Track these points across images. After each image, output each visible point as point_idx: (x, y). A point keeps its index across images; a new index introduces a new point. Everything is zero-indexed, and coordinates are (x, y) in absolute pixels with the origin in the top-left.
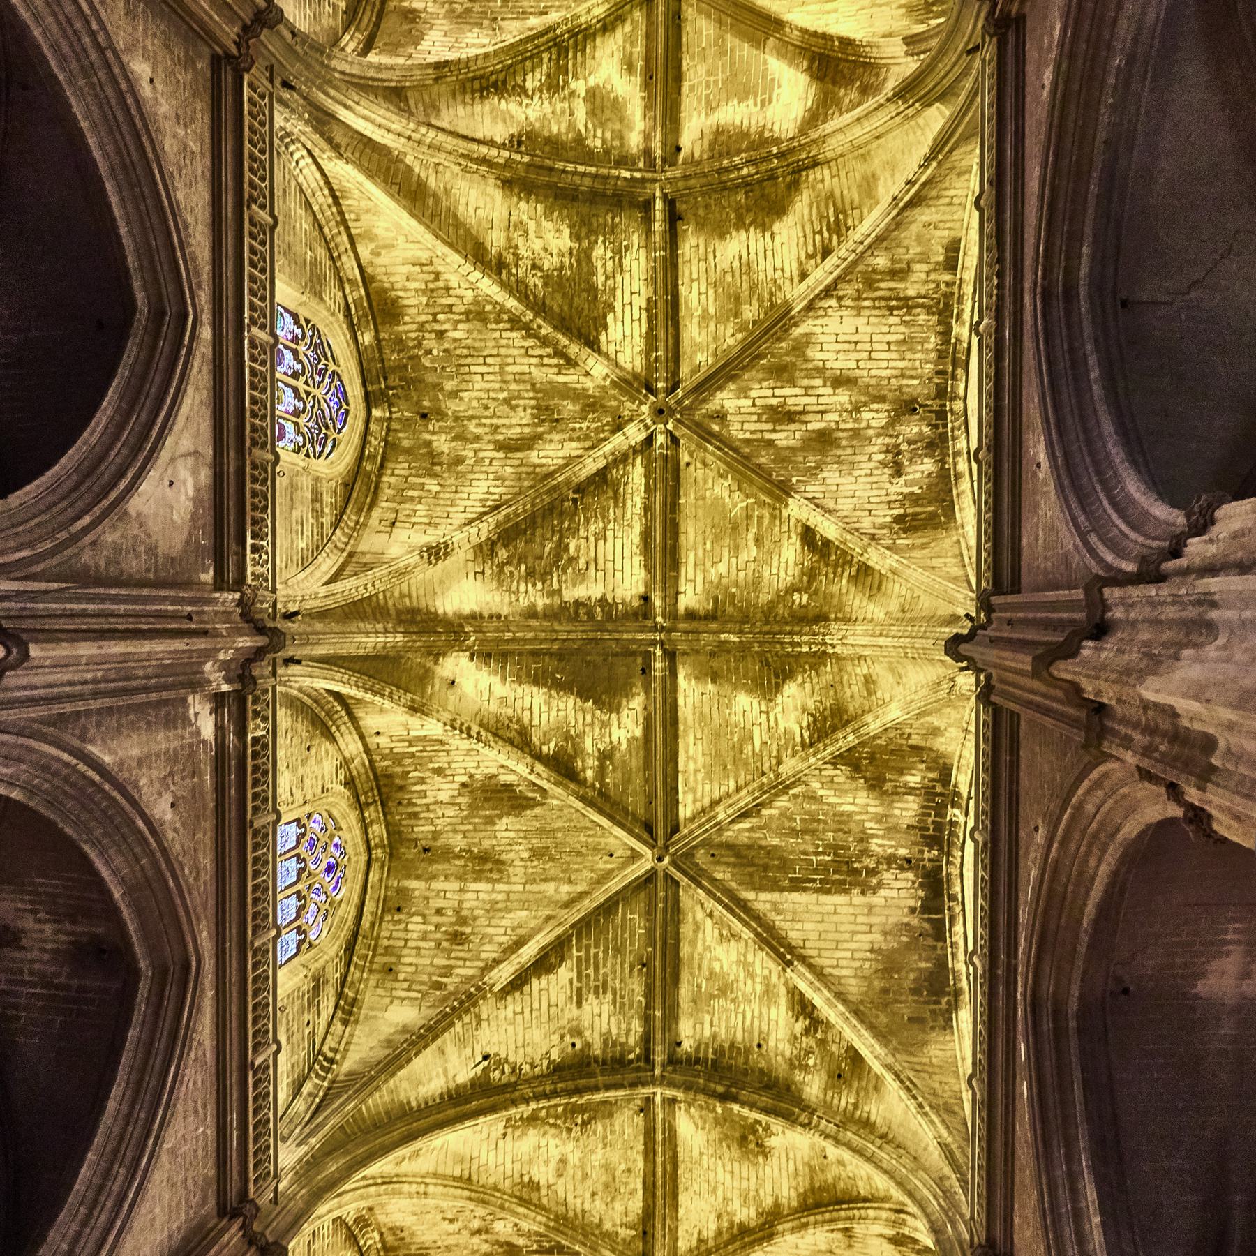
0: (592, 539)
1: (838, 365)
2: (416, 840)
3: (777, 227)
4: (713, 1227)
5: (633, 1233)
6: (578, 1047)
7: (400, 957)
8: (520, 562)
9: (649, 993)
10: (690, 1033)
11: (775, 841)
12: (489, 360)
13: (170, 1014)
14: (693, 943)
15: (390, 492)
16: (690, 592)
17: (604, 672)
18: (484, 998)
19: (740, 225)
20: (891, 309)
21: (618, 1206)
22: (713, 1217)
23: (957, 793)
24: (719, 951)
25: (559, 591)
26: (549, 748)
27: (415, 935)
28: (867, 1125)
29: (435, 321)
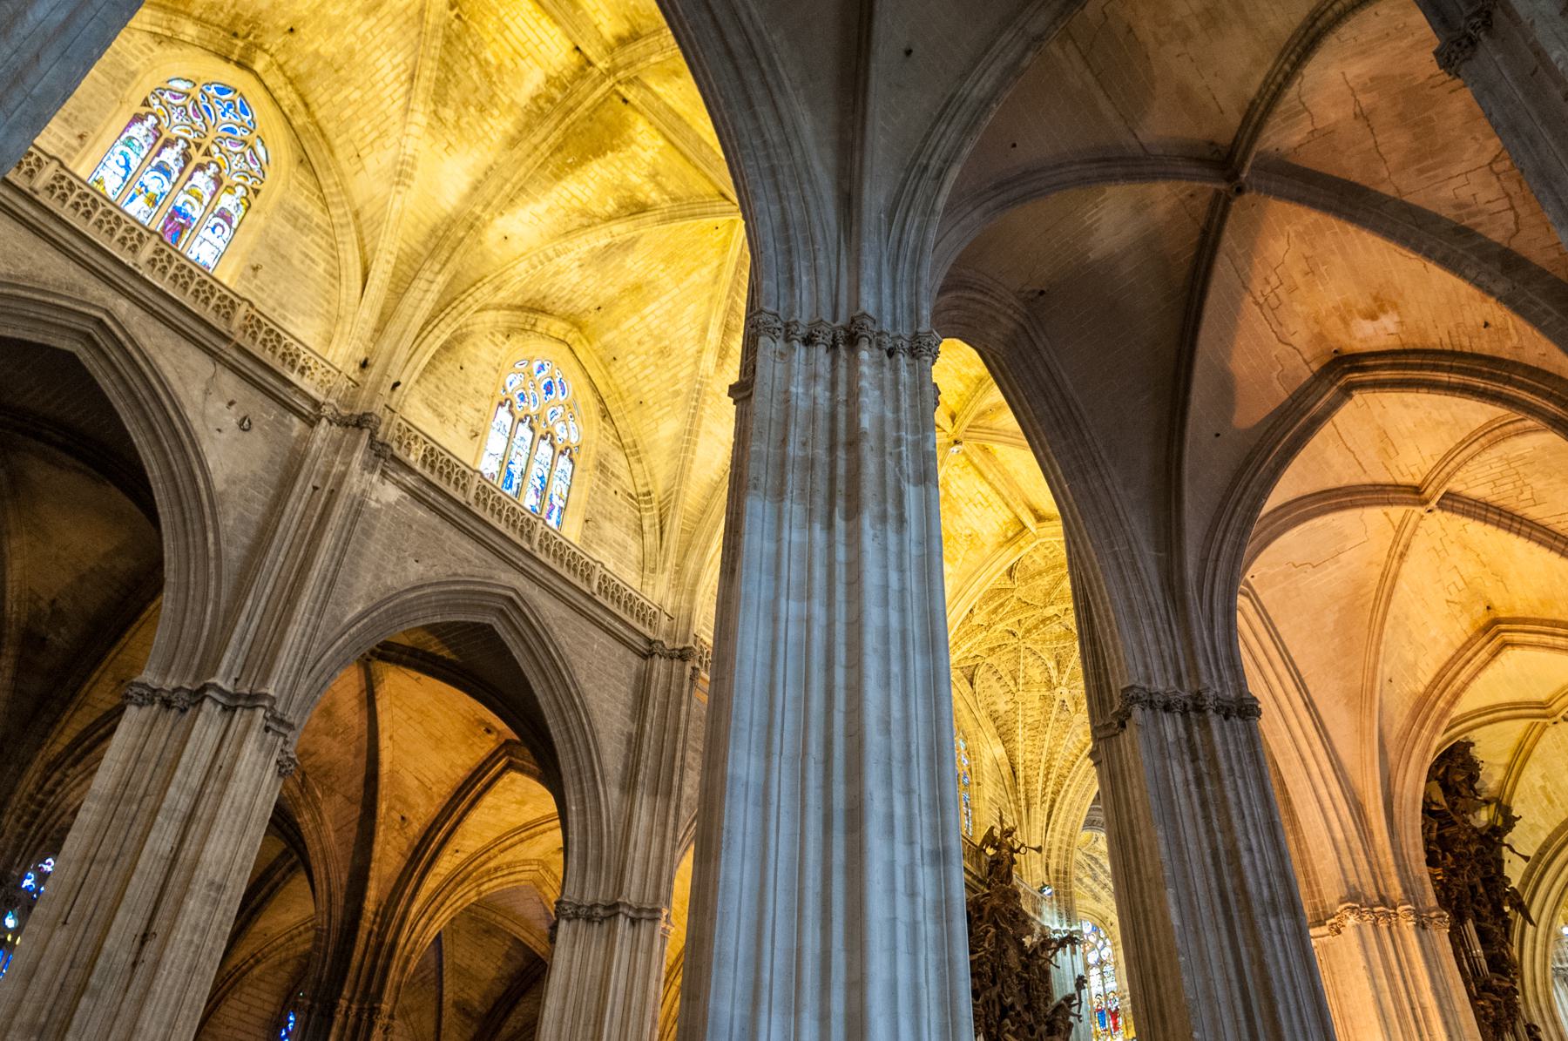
0: (498, 37)
7: (640, 390)
8: (466, 108)
13: (524, 626)
16: (604, 21)
17: (599, 127)
18: (708, 385)
22: (956, 381)
25: (513, 101)
26: (611, 206)
27: (638, 369)
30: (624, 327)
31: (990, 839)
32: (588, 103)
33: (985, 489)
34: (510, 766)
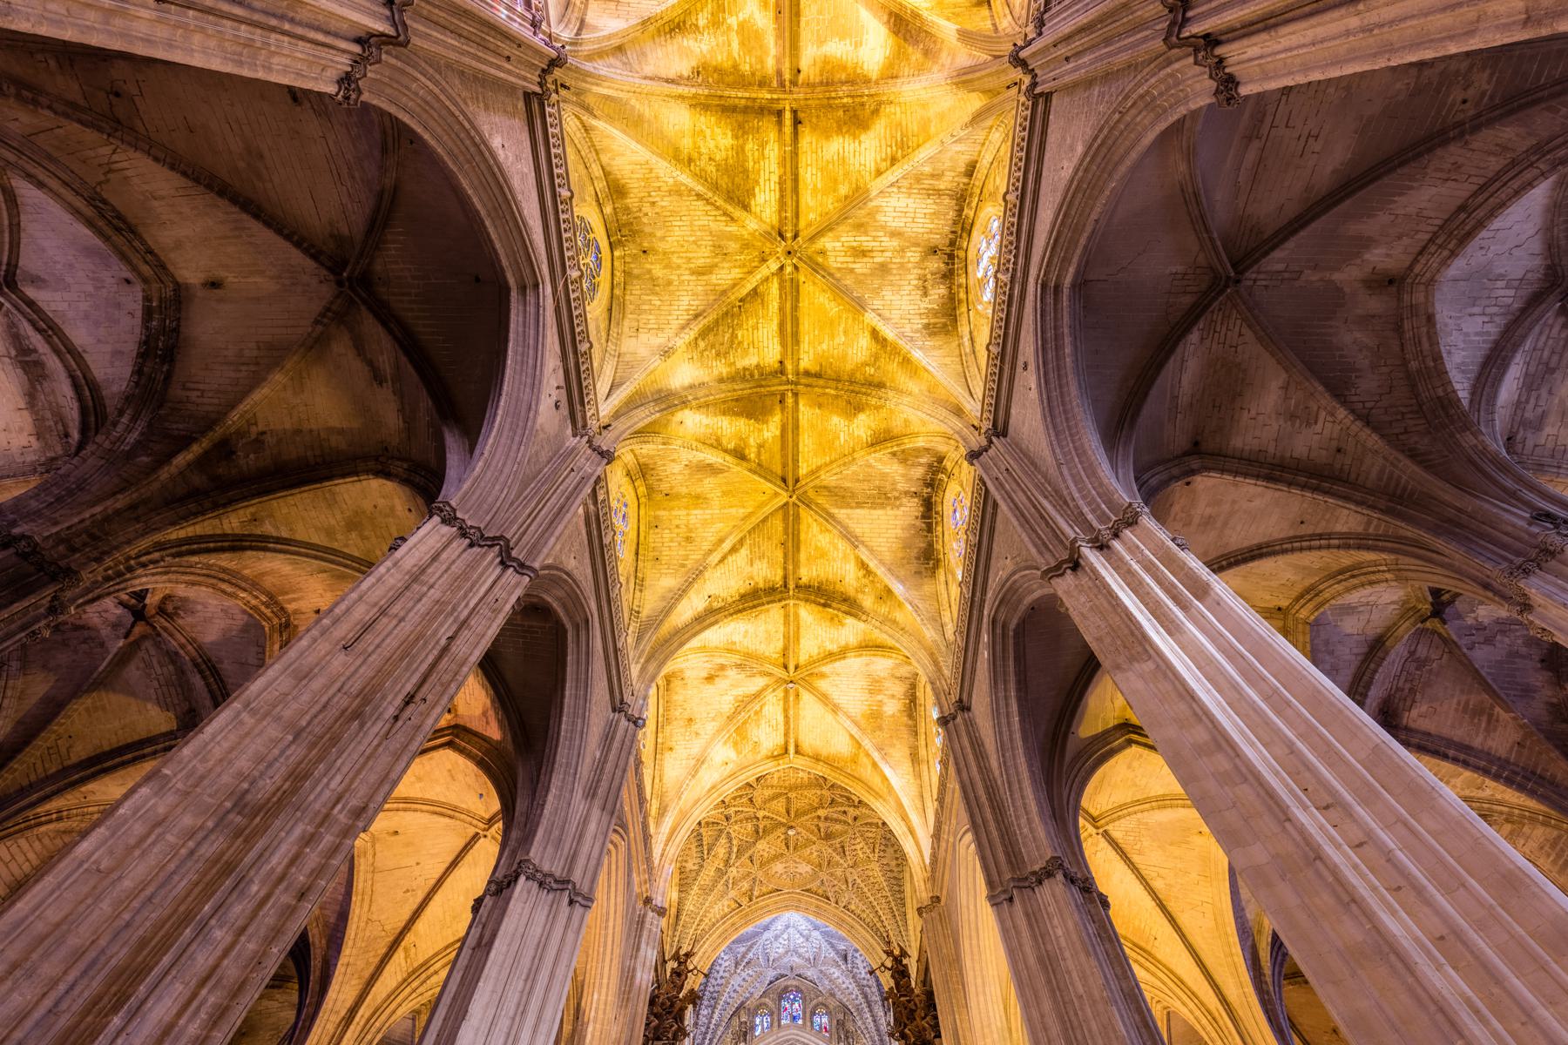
1: (894, 224)
3: (863, 137)
4: (816, 651)
10: (807, 574)
11: (849, 485)
14: (807, 533)
15: (632, 307)
16: (806, 360)
19: (839, 131)
20: (929, 195)
21: (772, 646)
24: (820, 537)
26: (731, 446)
28: (894, 622)
30: (674, 513)
31: (676, 957)
32: (773, 389)
33: (781, 719)
34: (449, 744)
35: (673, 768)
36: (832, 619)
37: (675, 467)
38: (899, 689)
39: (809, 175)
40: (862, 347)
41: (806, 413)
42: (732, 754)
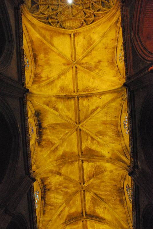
1: (59, 195)
2: (114, 126)
3: (68, 214)
4: (67, 74)
5: (79, 71)
6: (88, 99)
9: (78, 107)
10: (72, 102)
12: (107, 194)
16: (77, 164)
19: (73, 214)
23: (37, 141)
26: (95, 141)
28: (45, 98)
29: (114, 200)
33: (76, 47)
35: (112, 34)
36: (63, 89)
37: (111, 133)
38: (40, 62)
39: (79, 203)
40: (63, 171)
41: (76, 150)
42: (92, 35)
